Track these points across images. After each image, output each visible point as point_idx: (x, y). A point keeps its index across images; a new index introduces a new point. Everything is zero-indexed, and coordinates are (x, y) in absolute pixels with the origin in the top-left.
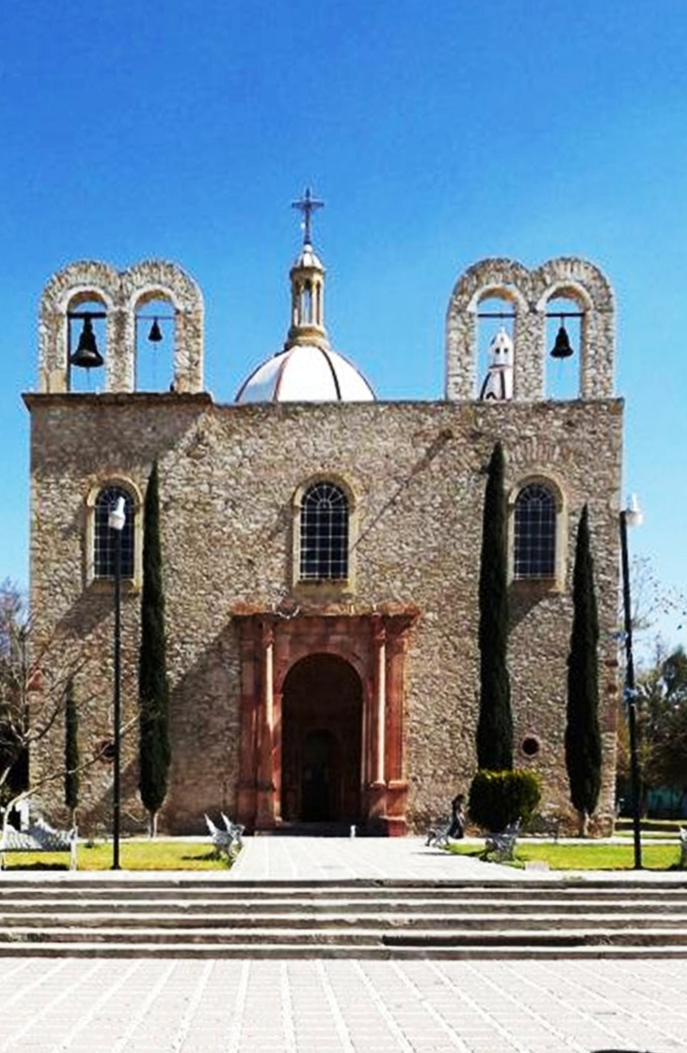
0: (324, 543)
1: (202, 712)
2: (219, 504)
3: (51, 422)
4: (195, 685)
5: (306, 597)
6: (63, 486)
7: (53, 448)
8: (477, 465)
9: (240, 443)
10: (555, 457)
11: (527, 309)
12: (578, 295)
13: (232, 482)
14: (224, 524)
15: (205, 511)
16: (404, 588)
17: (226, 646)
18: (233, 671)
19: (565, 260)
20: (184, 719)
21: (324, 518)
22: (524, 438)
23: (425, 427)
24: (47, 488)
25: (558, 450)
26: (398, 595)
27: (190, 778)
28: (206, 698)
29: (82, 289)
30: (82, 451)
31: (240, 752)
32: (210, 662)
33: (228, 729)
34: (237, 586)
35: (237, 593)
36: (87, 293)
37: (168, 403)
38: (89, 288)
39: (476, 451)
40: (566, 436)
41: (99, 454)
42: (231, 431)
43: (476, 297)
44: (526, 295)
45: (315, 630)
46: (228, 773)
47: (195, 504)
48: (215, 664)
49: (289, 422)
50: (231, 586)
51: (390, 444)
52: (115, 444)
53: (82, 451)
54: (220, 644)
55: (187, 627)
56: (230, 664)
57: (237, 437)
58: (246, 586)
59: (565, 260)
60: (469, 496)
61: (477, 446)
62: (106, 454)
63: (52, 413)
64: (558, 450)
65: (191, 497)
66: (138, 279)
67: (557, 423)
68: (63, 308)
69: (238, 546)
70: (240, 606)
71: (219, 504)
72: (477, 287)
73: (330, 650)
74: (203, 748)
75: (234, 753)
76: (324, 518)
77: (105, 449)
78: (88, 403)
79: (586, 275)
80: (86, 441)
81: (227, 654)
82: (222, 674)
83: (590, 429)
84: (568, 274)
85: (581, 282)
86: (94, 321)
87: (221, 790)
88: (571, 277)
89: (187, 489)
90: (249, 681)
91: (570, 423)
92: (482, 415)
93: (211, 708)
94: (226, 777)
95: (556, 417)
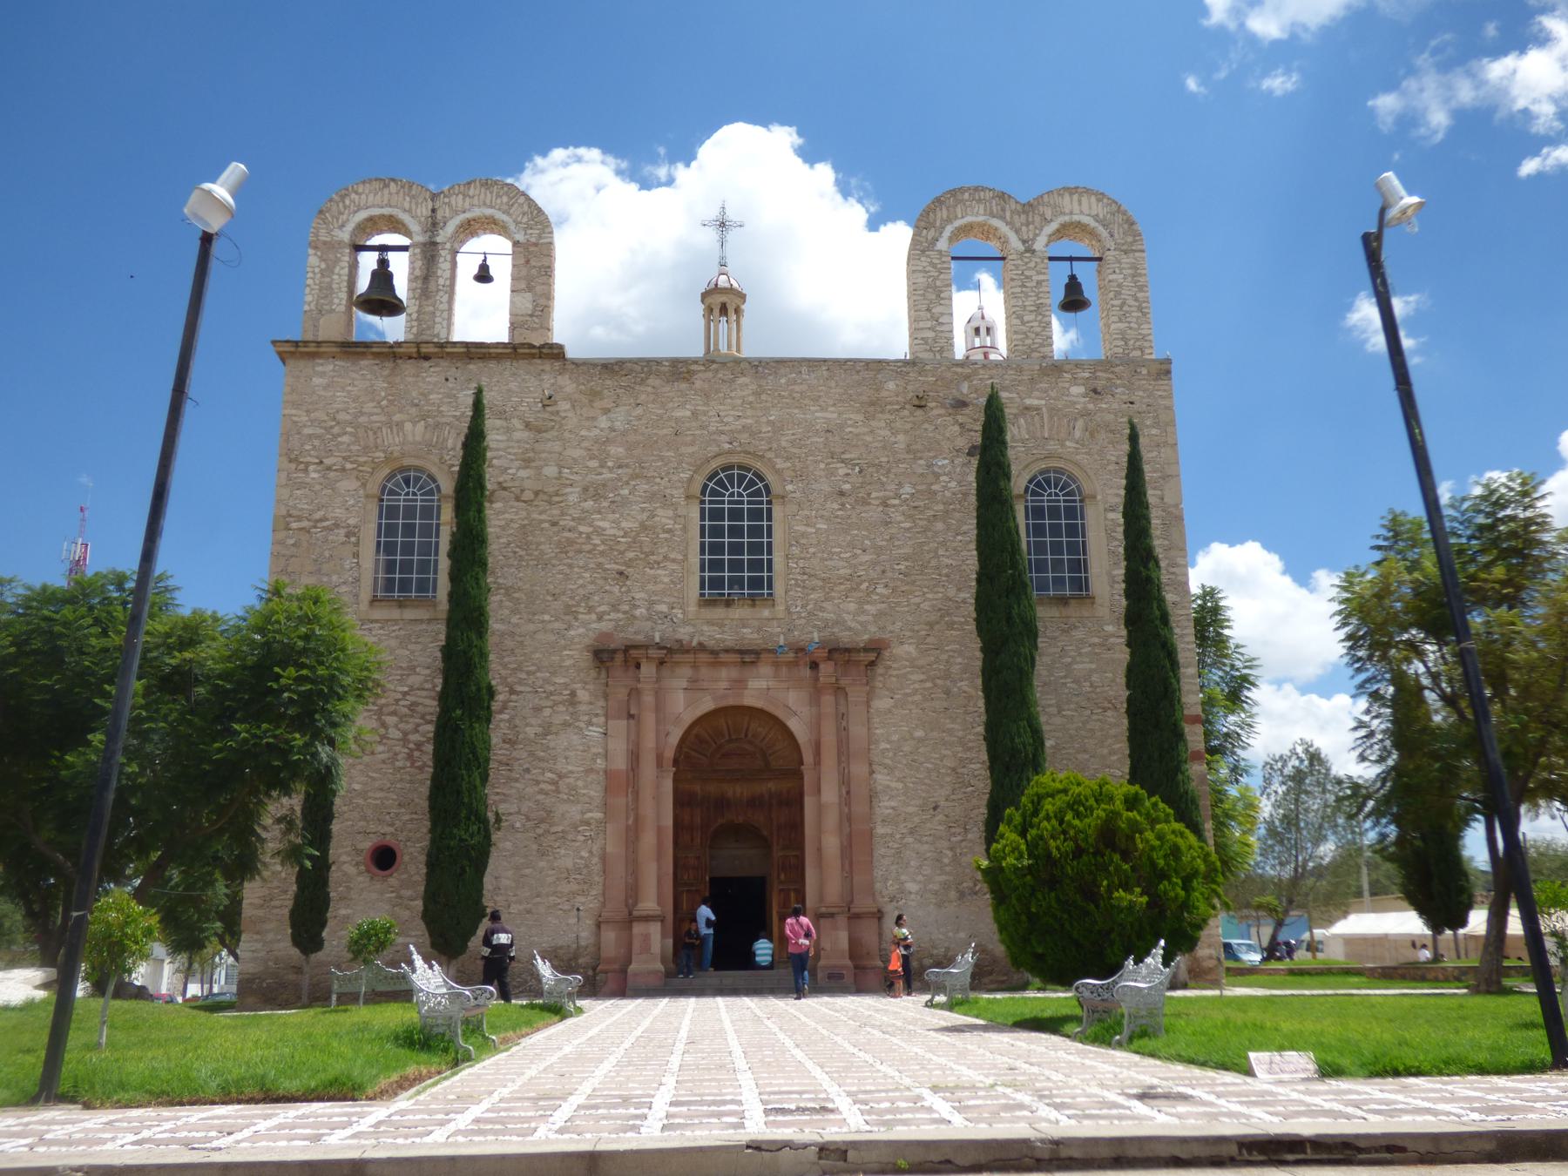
0: (736, 549)
1: (540, 797)
2: (573, 495)
3: (317, 381)
4: (531, 754)
5: (710, 623)
6: (329, 468)
7: (321, 415)
8: (962, 443)
9: (606, 411)
10: (1078, 434)
11: (1021, 248)
12: (1093, 234)
13: (594, 464)
14: (580, 520)
15: (550, 503)
16: (864, 612)
17: (583, 695)
18: (594, 732)
19: (1072, 191)
20: (514, 808)
21: (736, 514)
22: (1027, 408)
23: (884, 394)
24: (306, 470)
25: (1080, 424)
26: (853, 620)
27: (520, 903)
28: (549, 775)
29: (376, 212)
30: (361, 419)
31: (604, 858)
32: (558, 719)
33: (588, 823)
34: (602, 609)
35: (600, 619)
36: (382, 216)
37: (498, 357)
38: (386, 211)
39: (961, 425)
40: (1091, 406)
41: (390, 425)
42: (594, 395)
43: (949, 229)
44: (1017, 231)
45: (724, 673)
46: (583, 893)
47: (537, 493)
48: (566, 724)
49: (684, 386)
50: (590, 610)
51: (831, 415)
52: (413, 411)
53: (361, 419)
54: (573, 694)
55: (519, 669)
56: (590, 723)
57: (607, 403)
58: (614, 608)
59: (1072, 191)
60: (953, 484)
61: (960, 419)
62: (400, 425)
63: (319, 369)
64: (1080, 424)
65: (528, 484)
66: (458, 201)
67: (1077, 390)
68: (345, 235)
69: (602, 553)
70: (604, 635)
71: (573, 495)
72: (949, 221)
73: (749, 700)
74: (542, 854)
75: (595, 860)
76: (736, 514)
77: (397, 417)
78: (377, 355)
79: (1099, 209)
80: (369, 407)
81: (583, 708)
82: (575, 739)
83: (1125, 397)
84: (1076, 208)
85: (1096, 218)
86: (392, 257)
87: (573, 921)
88: (1084, 211)
89: (523, 473)
90: (619, 747)
91: (1095, 391)
92: (967, 377)
93: (558, 791)
94: (581, 899)
95: (1074, 381)
